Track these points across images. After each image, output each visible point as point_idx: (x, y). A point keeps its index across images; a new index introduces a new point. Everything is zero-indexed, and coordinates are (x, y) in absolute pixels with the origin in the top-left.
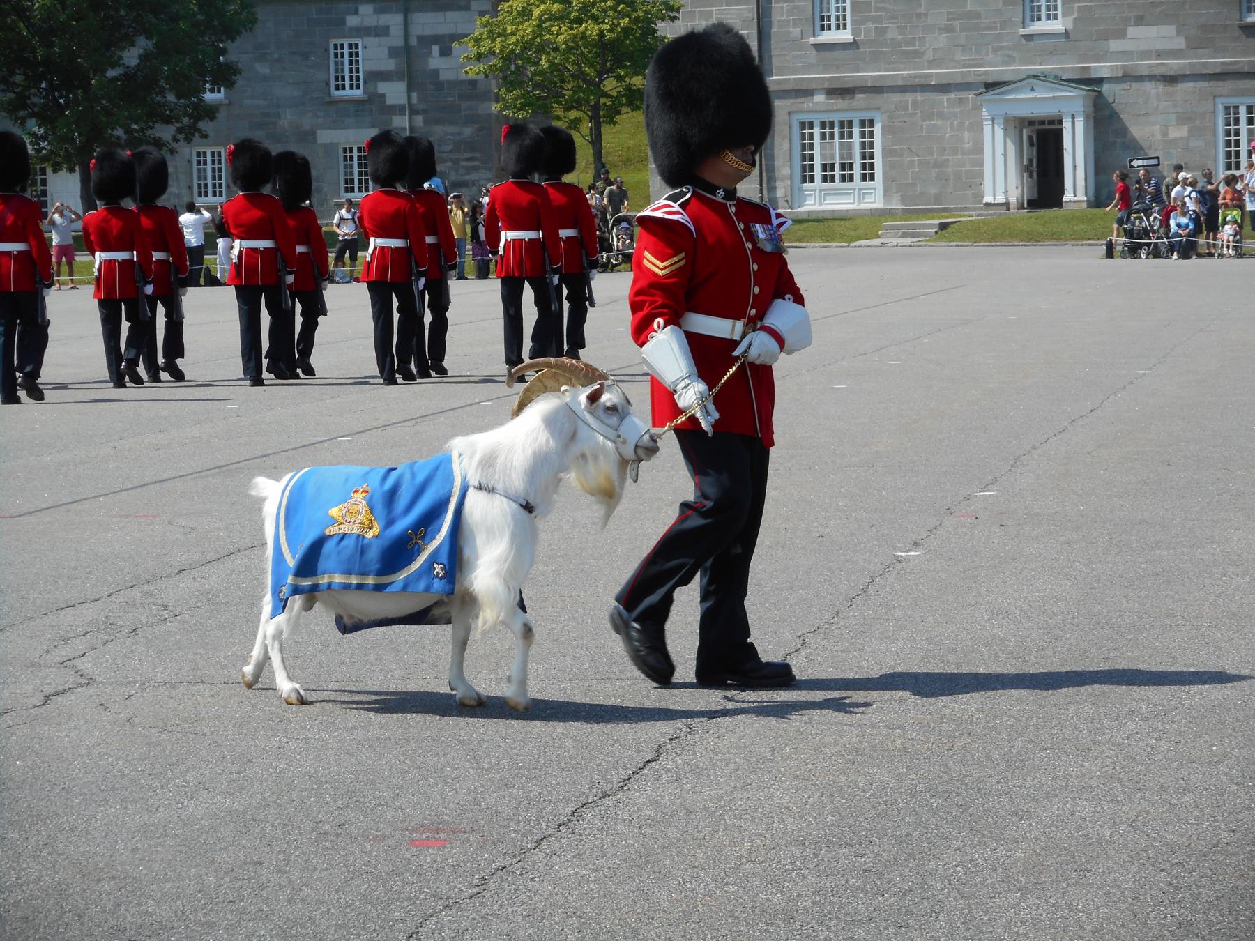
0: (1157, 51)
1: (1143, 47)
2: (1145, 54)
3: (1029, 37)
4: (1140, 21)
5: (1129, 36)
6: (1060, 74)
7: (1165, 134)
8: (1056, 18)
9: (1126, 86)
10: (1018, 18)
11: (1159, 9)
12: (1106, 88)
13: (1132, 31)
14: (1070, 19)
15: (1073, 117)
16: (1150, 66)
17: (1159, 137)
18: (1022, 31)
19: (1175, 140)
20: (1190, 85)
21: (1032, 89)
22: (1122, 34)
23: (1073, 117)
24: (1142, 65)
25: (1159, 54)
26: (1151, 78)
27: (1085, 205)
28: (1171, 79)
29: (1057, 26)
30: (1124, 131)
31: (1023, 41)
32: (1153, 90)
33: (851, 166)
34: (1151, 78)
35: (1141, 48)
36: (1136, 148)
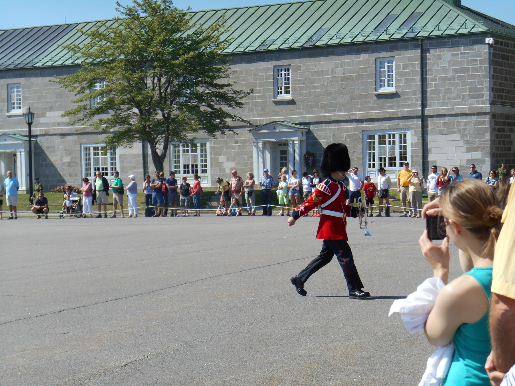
0: (58, 123)
1: (52, 120)
2: (54, 124)
3: (9, 117)
4: (51, 109)
5: (47, 115)
6: (21, 133)
7: (61, 160)
8: (20, 108)
9: (45, 138)
10: (6, 108)
11: (58, 104)
12: (39, 139)
13: (49, 114)
14: (25, 108)
15: (21, 152)
16: (54, 129)
17: (59, 162)
18: (7, 114)
19: (65, 163)
20: (70, 138)
21: (5, 140)
22: (44, 115)
23: (21, 152)
24: (52, 129)
25: (59, 124)
26: (56, 135)
27: (25, 192)
28: (63, 135)
29: (20, 112)
30: (46, 158)
31: (8, 118)
32: (57, 140)
33: (395, 159)
34: (56, 135)
35: (52, 121)
36: (51, 166)
